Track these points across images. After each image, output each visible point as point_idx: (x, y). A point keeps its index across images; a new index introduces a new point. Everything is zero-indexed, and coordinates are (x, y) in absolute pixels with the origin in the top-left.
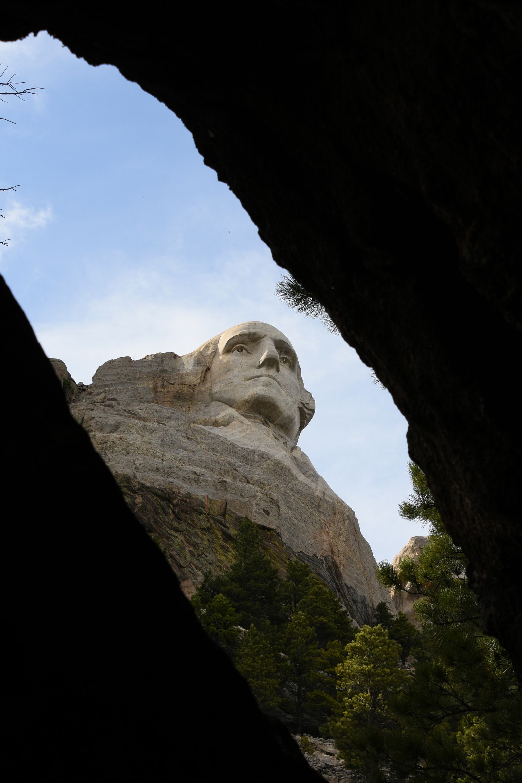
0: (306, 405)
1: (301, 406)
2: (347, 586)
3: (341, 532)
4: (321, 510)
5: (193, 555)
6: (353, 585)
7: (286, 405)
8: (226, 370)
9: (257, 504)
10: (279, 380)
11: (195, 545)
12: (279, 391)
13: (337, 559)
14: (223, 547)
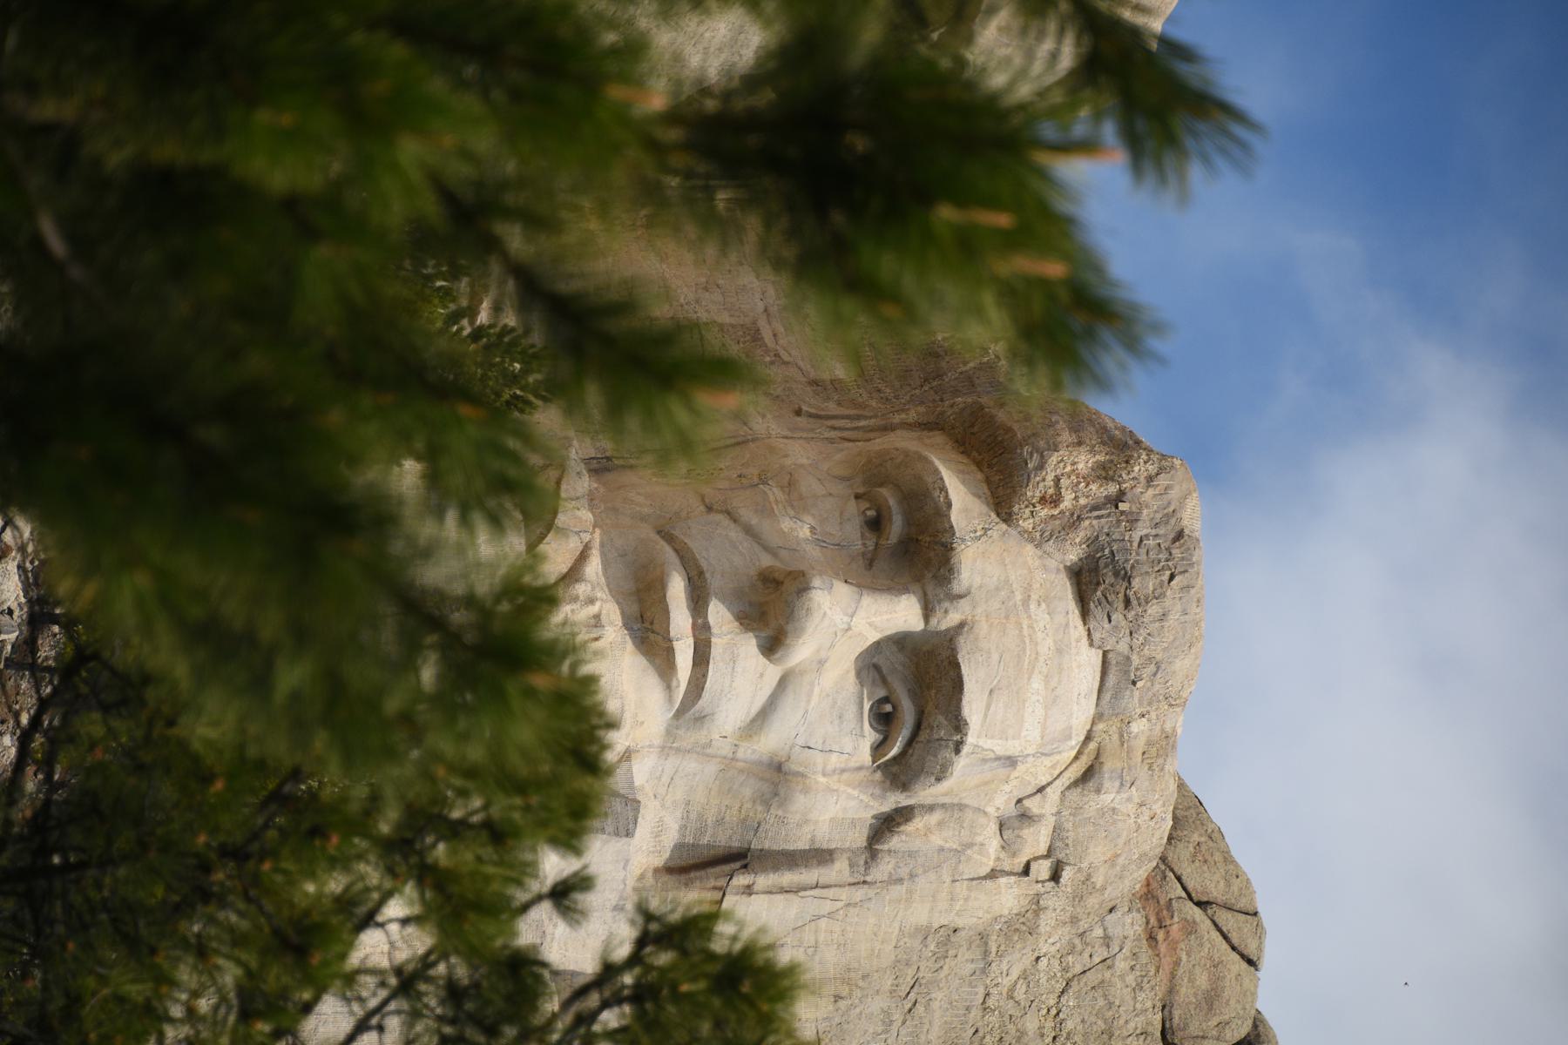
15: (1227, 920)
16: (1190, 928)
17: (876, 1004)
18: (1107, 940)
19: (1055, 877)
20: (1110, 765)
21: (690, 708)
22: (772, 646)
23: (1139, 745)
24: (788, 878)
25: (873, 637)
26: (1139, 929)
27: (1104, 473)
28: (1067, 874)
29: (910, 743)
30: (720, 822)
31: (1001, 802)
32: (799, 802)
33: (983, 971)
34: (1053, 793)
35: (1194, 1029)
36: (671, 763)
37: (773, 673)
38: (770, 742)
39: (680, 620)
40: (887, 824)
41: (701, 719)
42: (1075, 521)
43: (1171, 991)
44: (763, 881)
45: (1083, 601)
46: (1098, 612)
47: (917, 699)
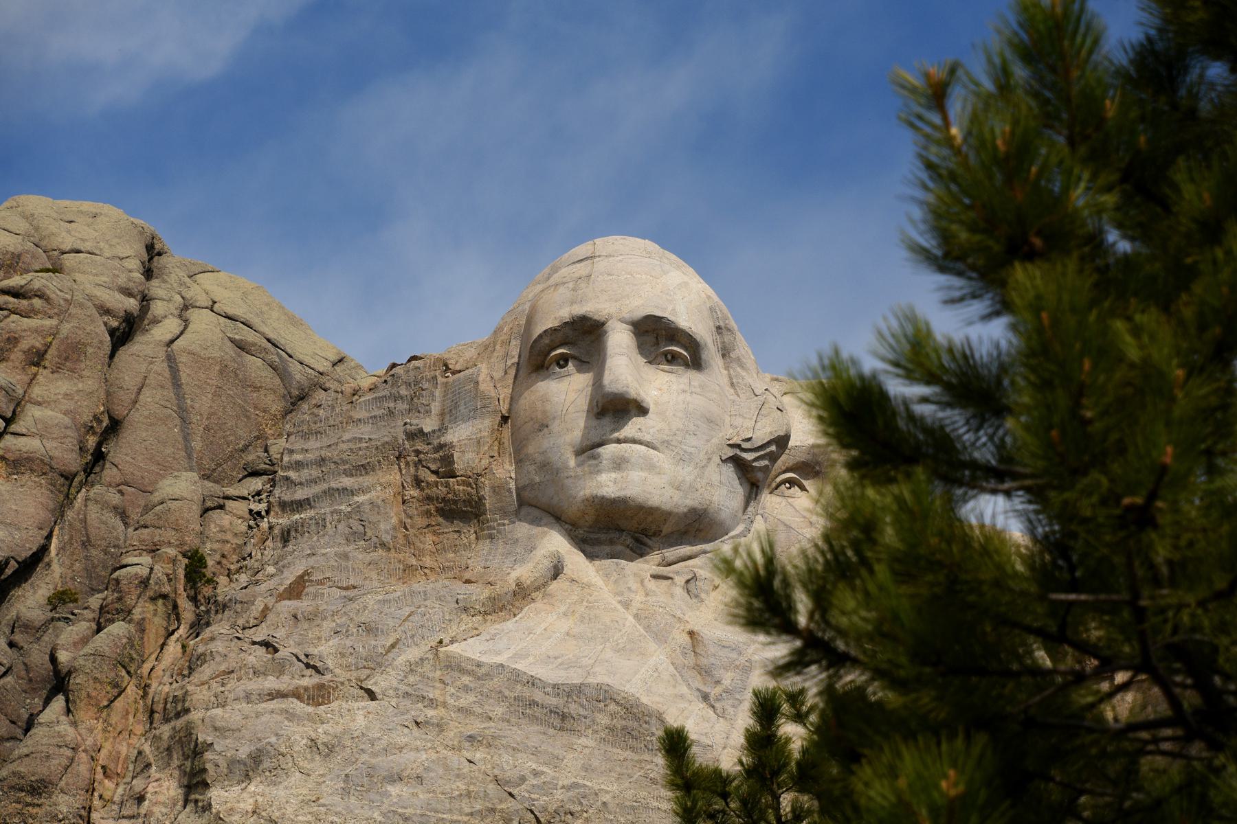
0: (745, 445)
1: (730, 452)
7: (678, 489)
8: (537, 426)
10: (647, 438)
12: (651, 467)
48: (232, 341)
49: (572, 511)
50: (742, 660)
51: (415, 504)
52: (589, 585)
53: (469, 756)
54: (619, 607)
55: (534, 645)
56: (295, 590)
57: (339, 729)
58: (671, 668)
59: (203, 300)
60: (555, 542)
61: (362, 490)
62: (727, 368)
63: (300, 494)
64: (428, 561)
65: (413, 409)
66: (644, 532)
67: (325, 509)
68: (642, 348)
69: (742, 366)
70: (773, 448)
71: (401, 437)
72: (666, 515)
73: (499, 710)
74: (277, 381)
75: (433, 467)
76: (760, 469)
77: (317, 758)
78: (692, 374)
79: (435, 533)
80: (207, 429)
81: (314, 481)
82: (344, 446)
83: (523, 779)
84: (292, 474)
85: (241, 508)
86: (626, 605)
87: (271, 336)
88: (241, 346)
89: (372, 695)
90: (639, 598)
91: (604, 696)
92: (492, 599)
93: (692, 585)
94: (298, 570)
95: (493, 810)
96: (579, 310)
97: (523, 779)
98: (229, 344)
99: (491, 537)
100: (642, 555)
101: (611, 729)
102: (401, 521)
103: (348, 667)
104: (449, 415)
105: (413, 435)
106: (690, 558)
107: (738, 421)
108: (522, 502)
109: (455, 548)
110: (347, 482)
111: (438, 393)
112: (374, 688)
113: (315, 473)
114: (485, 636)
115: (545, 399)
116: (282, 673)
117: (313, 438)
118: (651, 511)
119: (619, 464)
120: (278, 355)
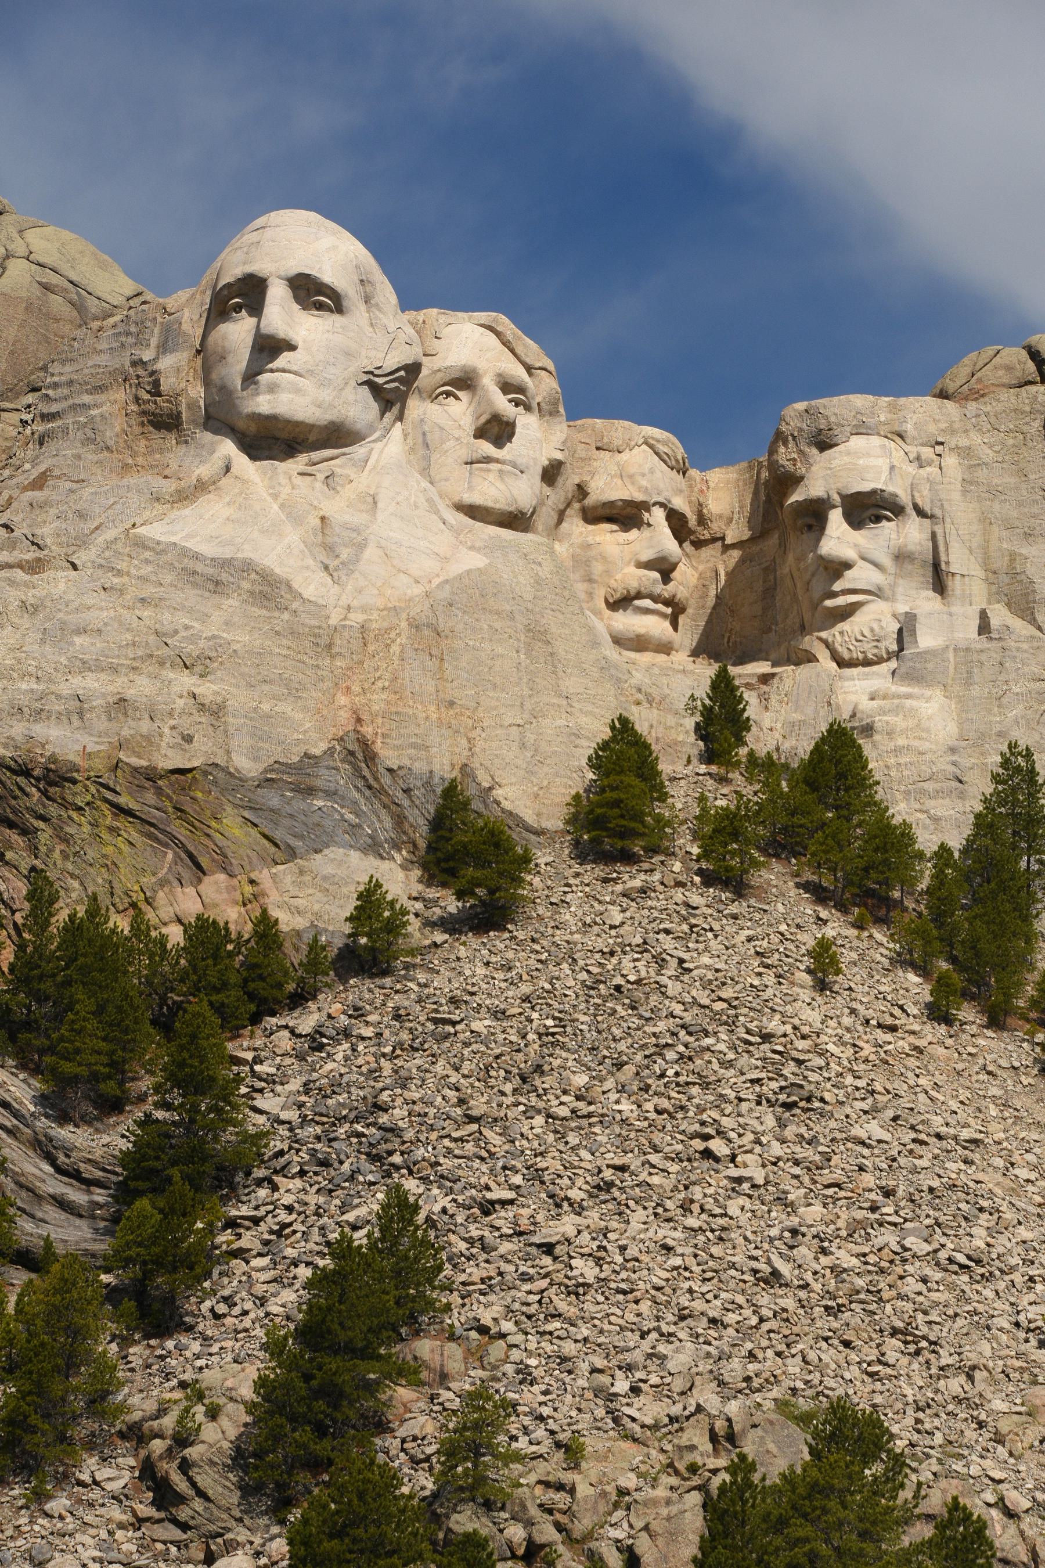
0: (377, 372)
1: (365, 377)
2: (390, 770)
3: (378, 675)
4: (336, 650)
5: (65, 856)
6: (406, 762)
9: (173, 728)
10: (295, 368)
11: (66, 839)
12: (297, 390)
13: (367, 730)
14: (113, 830)
15: (980, 364)
16: (980, 381)
17: (996, 506)
18: (977, 416)
19: (942, 444)
20: (897, 428)
21: (877, 593)
22: (848, 566)
23: (890, 416)
24: (942, 548)
25: (845, 526)
26: (974, 403)
27: (785, 443)
28: (940, 439)
29: (886, 509)
30: (924, 576)
31: (911, 469)
32: (911, 547)
33: (986, 464)
34: (907, 448)
35: (1019, 374)
36: (899, 597)
37: (861, 563)
38: (887, 561)
39: (841, 601)
40: (920, 513)
41: (880, 589)
42: (801, 452)
43: (1004, 385)
44: (943, 558)
45: (831, 446)
46: (835, 440)
47: (867, 509)
48: (39, 283)
49: (241, 425)
50: (359, 538)
51: (135, 417)
52: (246, 482)
53: (138, 612)
54: (269, 499)
55: (201, 528)
56: (39, 483)
57: (44, 593)
58: (302, 546)
59: (22, 251)
60: (228, 447)
61: (96, 406)
62: (368, 312)
63: (54, 408)
64: (140, 460)
65: (140, 343)
66: (295, 440)
67: (69, 420)
68: (298, 299)
69: (380, 310)
70: (402, 373)
71: (128, 364)
72: (313, 426)
73: (169, 578)
74: (76, 313)
75: (148, 388)
76: (391, 390)
77: (26, 615)
78: (336, 318)
79: (147, 439)
80: (12, 353)
81: (65, 398)
82: (87, 371)
83: (176, 632)
84: (50, 392)
85: (15, 417)
86: (275, 496)
87: (74, 278)
88: (46, 287)
89: (75, 567)
90: (287, 490)
91: (248, 567)
92: (178, 492)
93: (330, 480)
94: (42, 468)
95: (151, 656)
96: (249, 269)
97: (176, 632)
98: (36, 285)
99: (186, 442)
100: (293, 457)
101: (252, 593)
102: (123, 430)
103: (60, 545)
104: (164, 348)
105: (134, 364)
106: (332, 459)
107: (373, 353)
108: (208, 417)
109: (161, 451)
110: (87, 399)
111: (156, 331)
112: (76, 562)
113: (66, 391)
114: (167, 520)
115: (224, 338)
116: (14, 549)
117: (68, 364)
118: (298, 424)
119: (272, 388)
120: (78, 294)
